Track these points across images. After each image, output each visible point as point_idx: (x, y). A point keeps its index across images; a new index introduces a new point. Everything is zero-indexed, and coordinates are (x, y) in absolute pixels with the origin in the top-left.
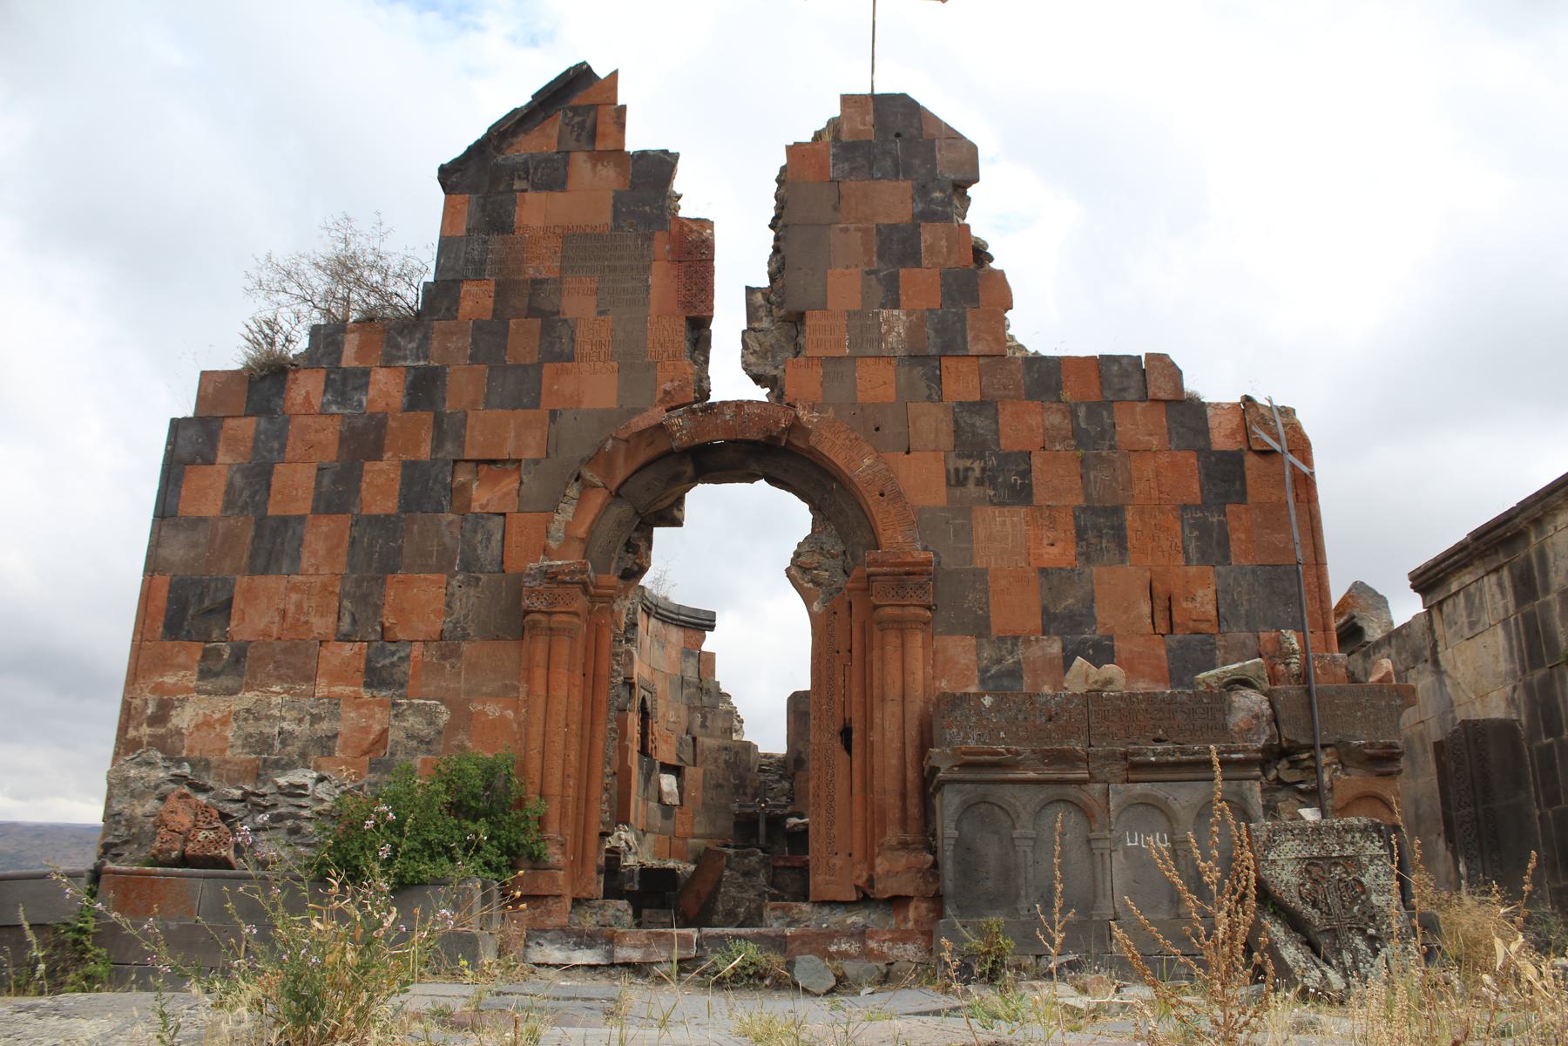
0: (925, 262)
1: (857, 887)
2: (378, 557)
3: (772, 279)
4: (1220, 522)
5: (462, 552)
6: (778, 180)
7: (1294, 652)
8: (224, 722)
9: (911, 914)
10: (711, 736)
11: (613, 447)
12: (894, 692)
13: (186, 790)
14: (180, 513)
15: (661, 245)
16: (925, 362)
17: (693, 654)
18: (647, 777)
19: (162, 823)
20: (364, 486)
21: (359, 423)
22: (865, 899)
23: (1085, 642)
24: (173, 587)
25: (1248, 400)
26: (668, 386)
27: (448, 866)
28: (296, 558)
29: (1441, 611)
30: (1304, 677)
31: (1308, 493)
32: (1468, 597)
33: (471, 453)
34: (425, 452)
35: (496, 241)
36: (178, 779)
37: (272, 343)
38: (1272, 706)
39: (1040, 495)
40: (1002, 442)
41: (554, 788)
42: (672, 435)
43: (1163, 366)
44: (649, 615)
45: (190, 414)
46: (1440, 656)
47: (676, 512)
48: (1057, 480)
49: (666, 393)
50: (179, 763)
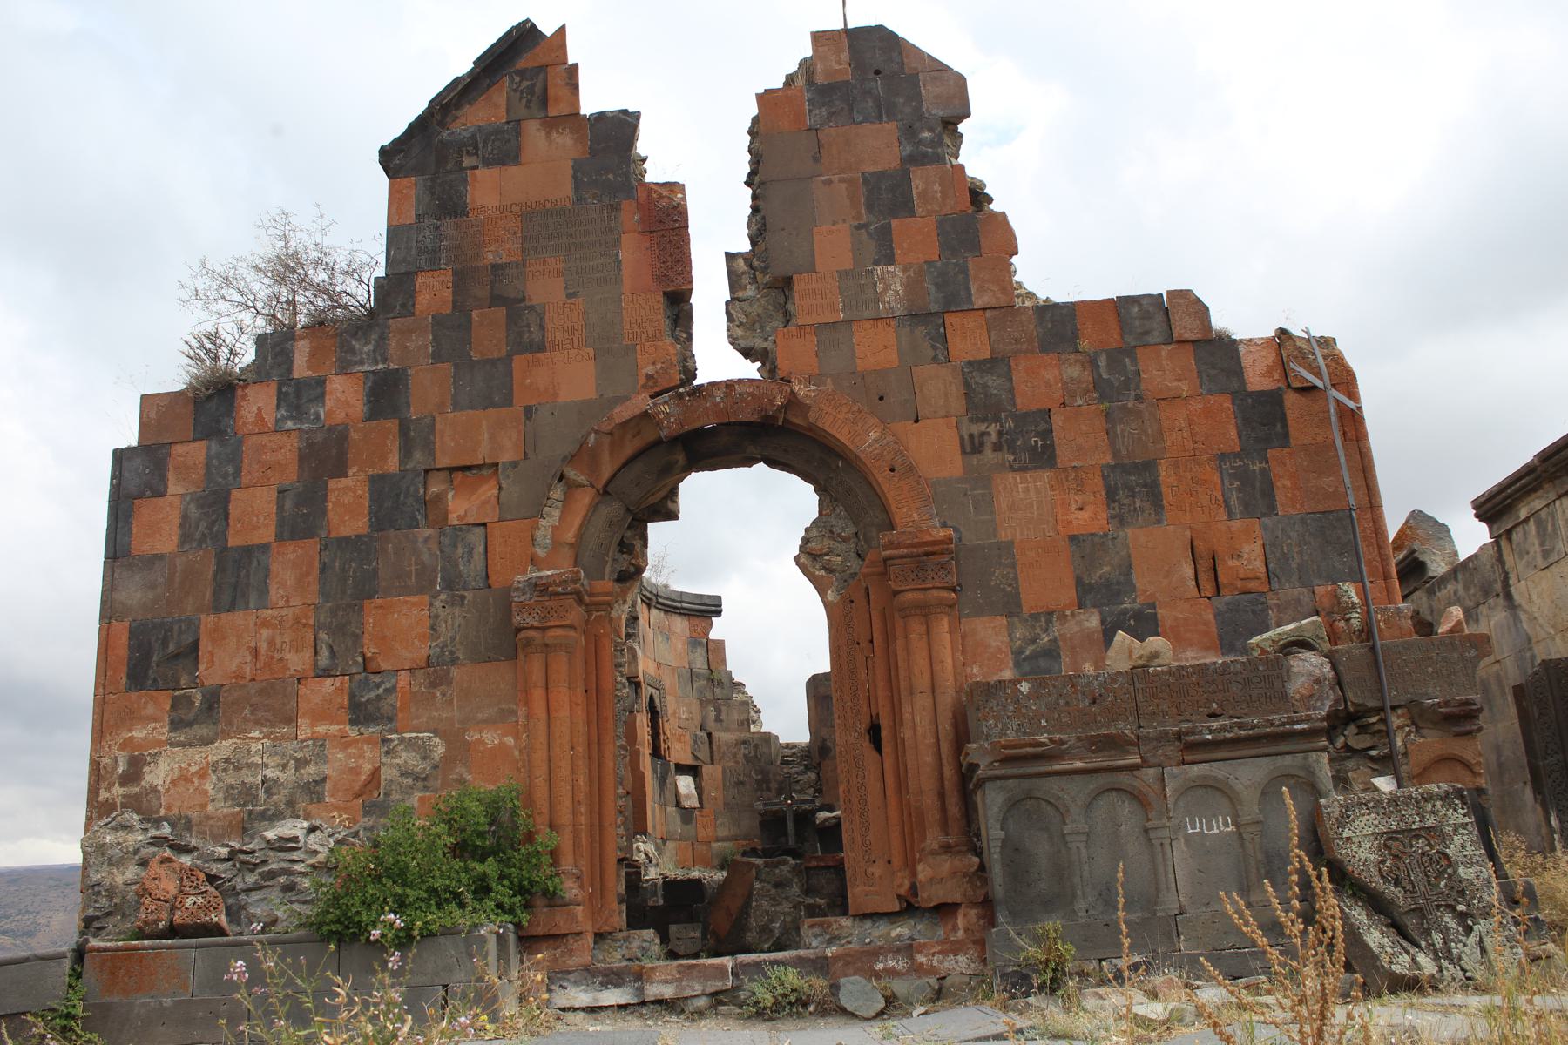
0: (918, 211)
1: (899, 897)
2: (352, 580)
3: (753, 243)
4: (1264, 472)
5: (443, 569)
6: (750, 132)
7: (1354, 606)
8: (202, 775)
9: (960, 921)
10: (727, 730)
12: (922, 682)
13: (168, 853)
14: (133, 552)
15: (630, 215)
16: (928, 319)
17: (700, 644)
18: (663, 781)
19: (146, 892)
20: (330, 506)
21: (319, 437)
22: (909, 908)
23: (1124, 612)
24: (133, 634)
25: (1283, 333)
26: (650, 370)
27: (457, 913)
28: (264, 591)
29: (1510, 540)
30: (1366, 633)
31: (1356, 430)
32: (1539, 523)
33: (443, 461)
34: (393, 464)
36: (158, 841)
37: (216, 358)
38: (1334, 668)
39: (1064, 455)
40: (1018, 401)
41: (565, 816)
42: (659, 424)
43: (1188, 304)
44: (649, 606)
45: (134, 443)
46: (1513, 589)
47: (670, 505)
48: (1081, 438)
49: (649, 377)
50: (157, 823)
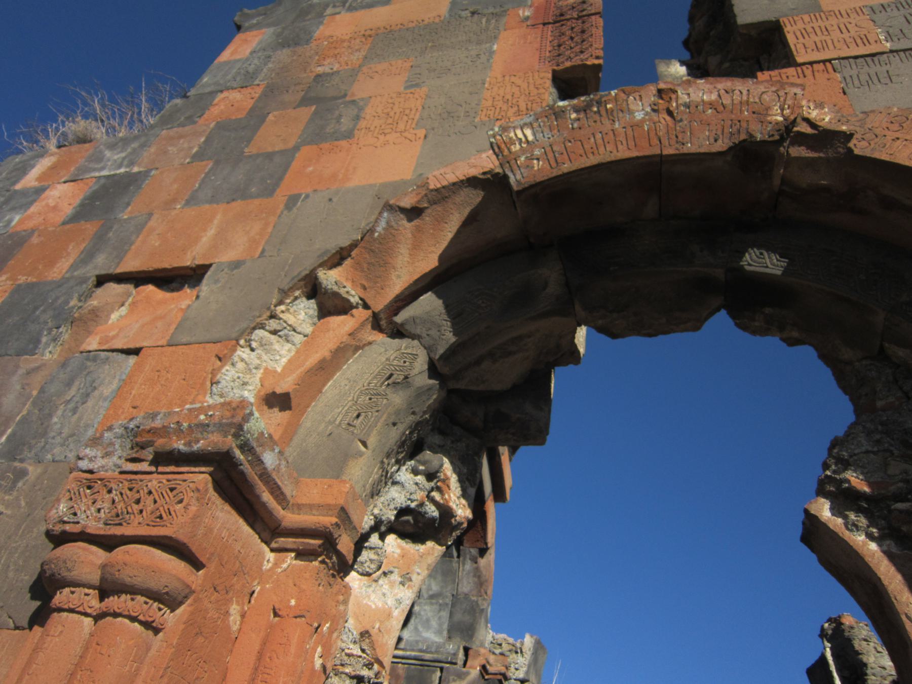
11: (389, 226)
33: (131, 265)
35: (284, 55)
